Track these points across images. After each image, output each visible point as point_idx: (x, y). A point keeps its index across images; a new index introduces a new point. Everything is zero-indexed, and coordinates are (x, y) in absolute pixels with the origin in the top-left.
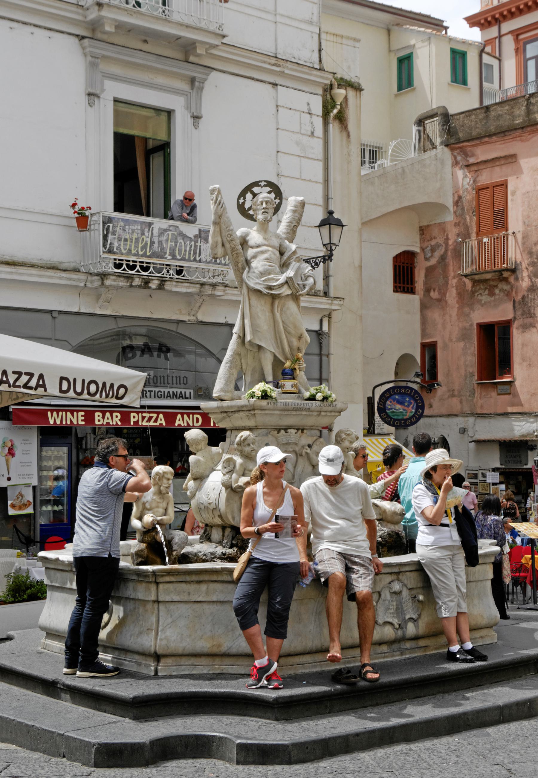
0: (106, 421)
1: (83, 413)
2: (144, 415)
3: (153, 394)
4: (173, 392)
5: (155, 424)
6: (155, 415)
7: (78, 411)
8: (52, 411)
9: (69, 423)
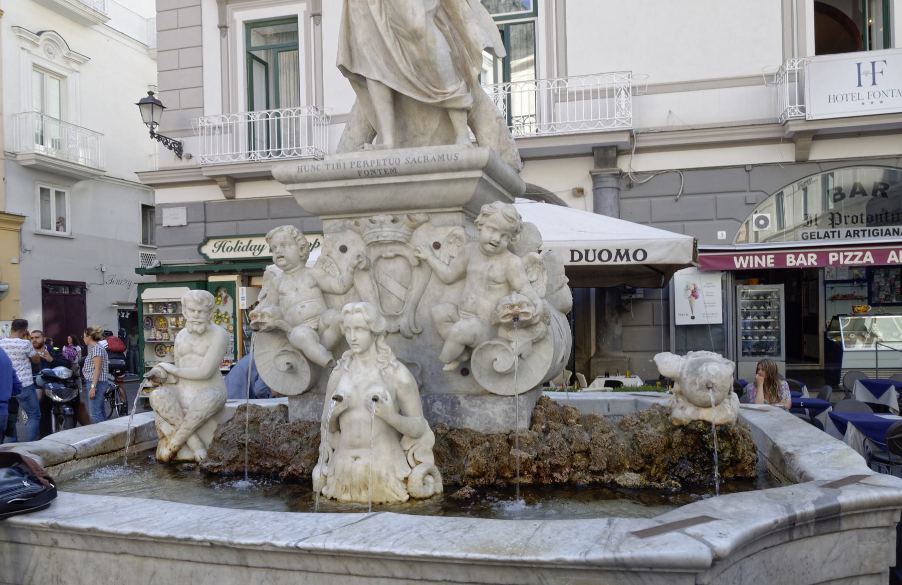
0: (799, 262)
1: (773, 256)
2: (846, 254)
3: (867, 233)
4: (894, 230)
5: (860, 262)
6: (861, 254)
7: (766, 255)
8: (738, 257)
9: (756, 266)
